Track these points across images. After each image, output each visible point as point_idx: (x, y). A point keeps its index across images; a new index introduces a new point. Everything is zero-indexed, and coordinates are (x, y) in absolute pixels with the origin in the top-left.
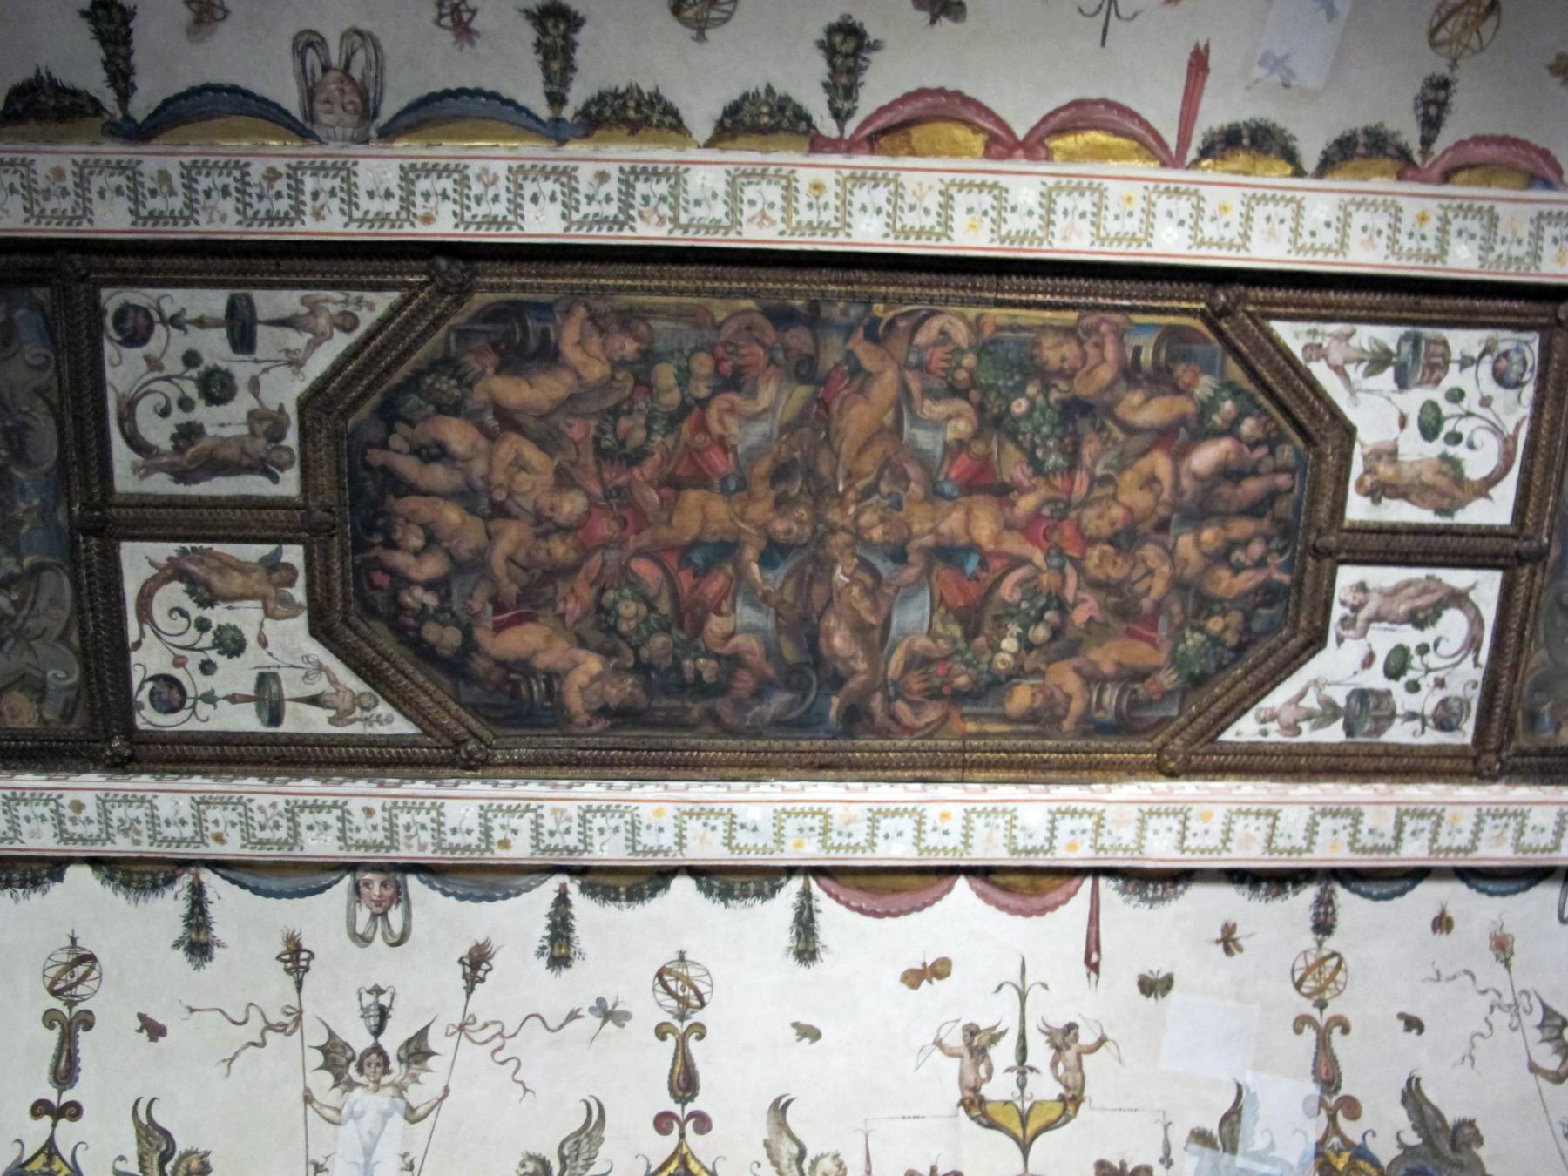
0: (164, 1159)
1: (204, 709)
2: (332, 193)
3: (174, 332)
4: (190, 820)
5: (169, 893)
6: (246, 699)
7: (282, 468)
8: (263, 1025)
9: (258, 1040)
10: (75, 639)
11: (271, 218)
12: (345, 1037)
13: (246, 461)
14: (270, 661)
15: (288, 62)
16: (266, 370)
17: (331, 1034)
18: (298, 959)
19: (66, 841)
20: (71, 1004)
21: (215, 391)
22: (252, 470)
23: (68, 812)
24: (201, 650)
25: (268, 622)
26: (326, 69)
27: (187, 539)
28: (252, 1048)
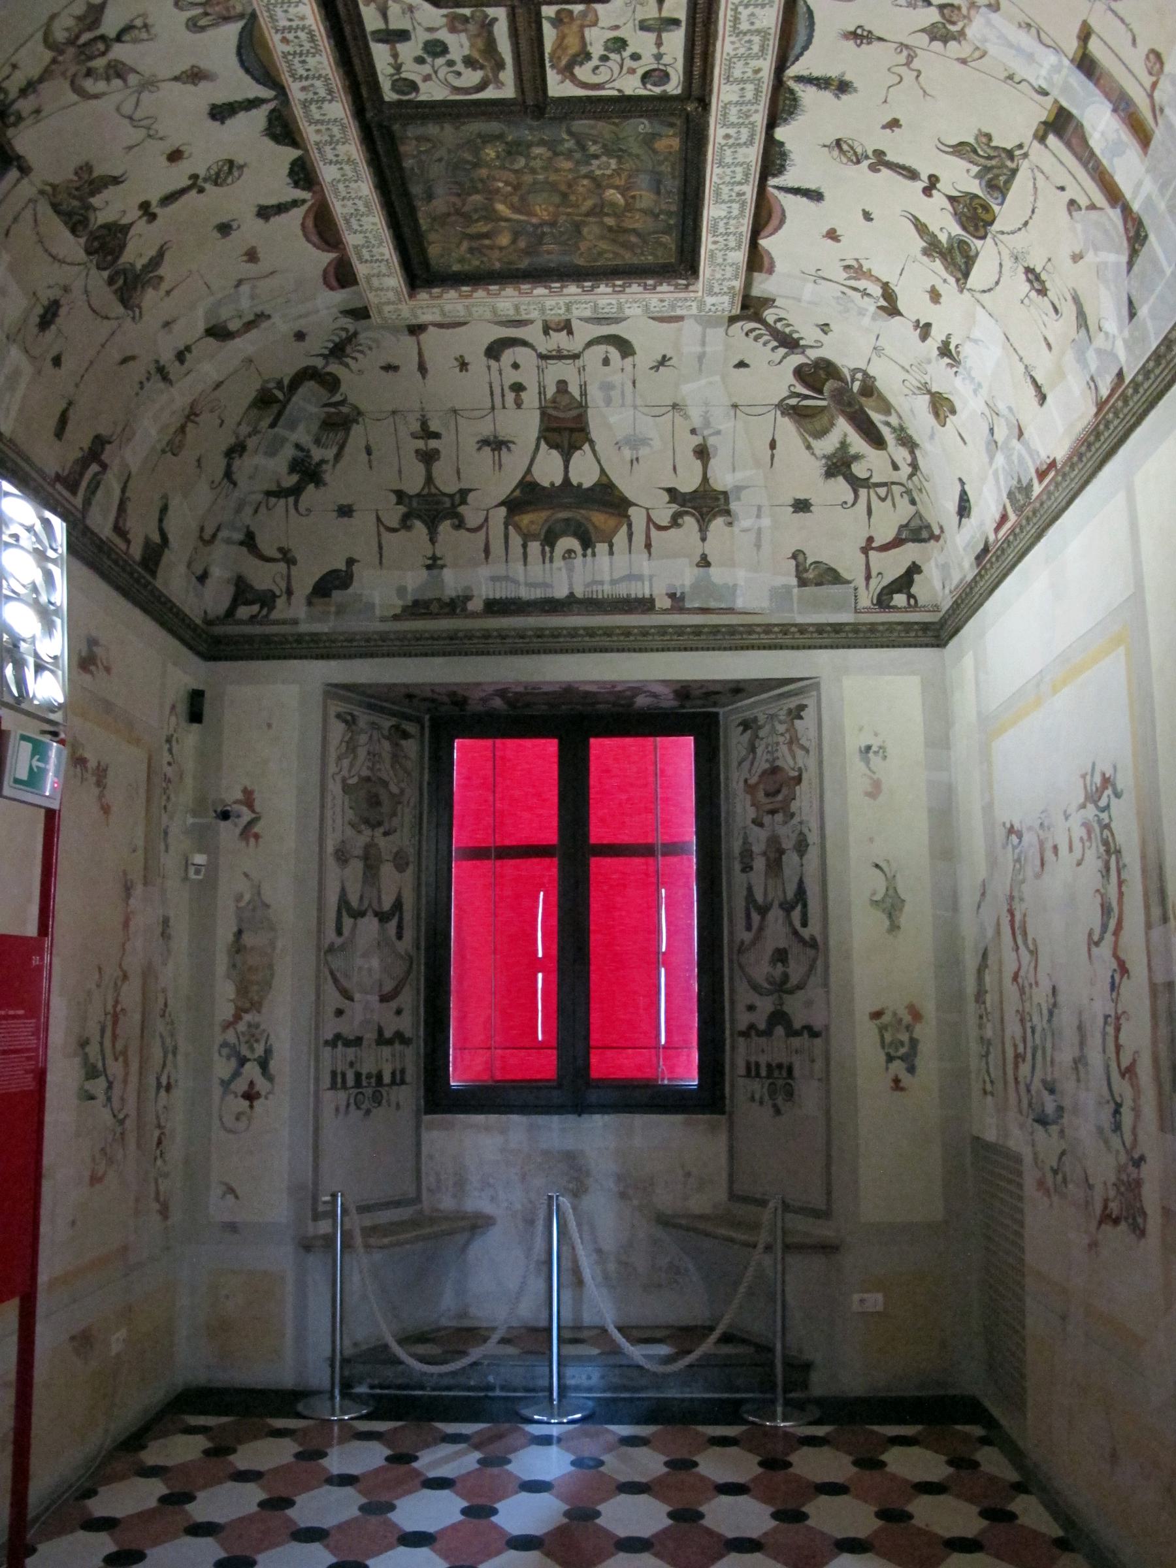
0: (975, 151)
1: (666, 59)
2: (286, 11)
3: (403, 69)
4: (741, 86)
5: (800, 94)
6: (659, 37)
7: (486, 16)
8: (905, 68)
9: (915, 74)
10: (617, 121)
11: (312, 39)
12: (926, 24)
13: (485, 34)
14: (630, 24)
15: (211, 33)
16: (419, 24)
17: (923, 30)
18: (862, 36)
19: (752, 143)
20: (867, 157)
21: (439, 50)
22: (490, 34)
23: (731, 141)
24: (623, 60)
25: (600, 24)
26: (206, 14)
27: (543, 66)
28: (920, 78)
